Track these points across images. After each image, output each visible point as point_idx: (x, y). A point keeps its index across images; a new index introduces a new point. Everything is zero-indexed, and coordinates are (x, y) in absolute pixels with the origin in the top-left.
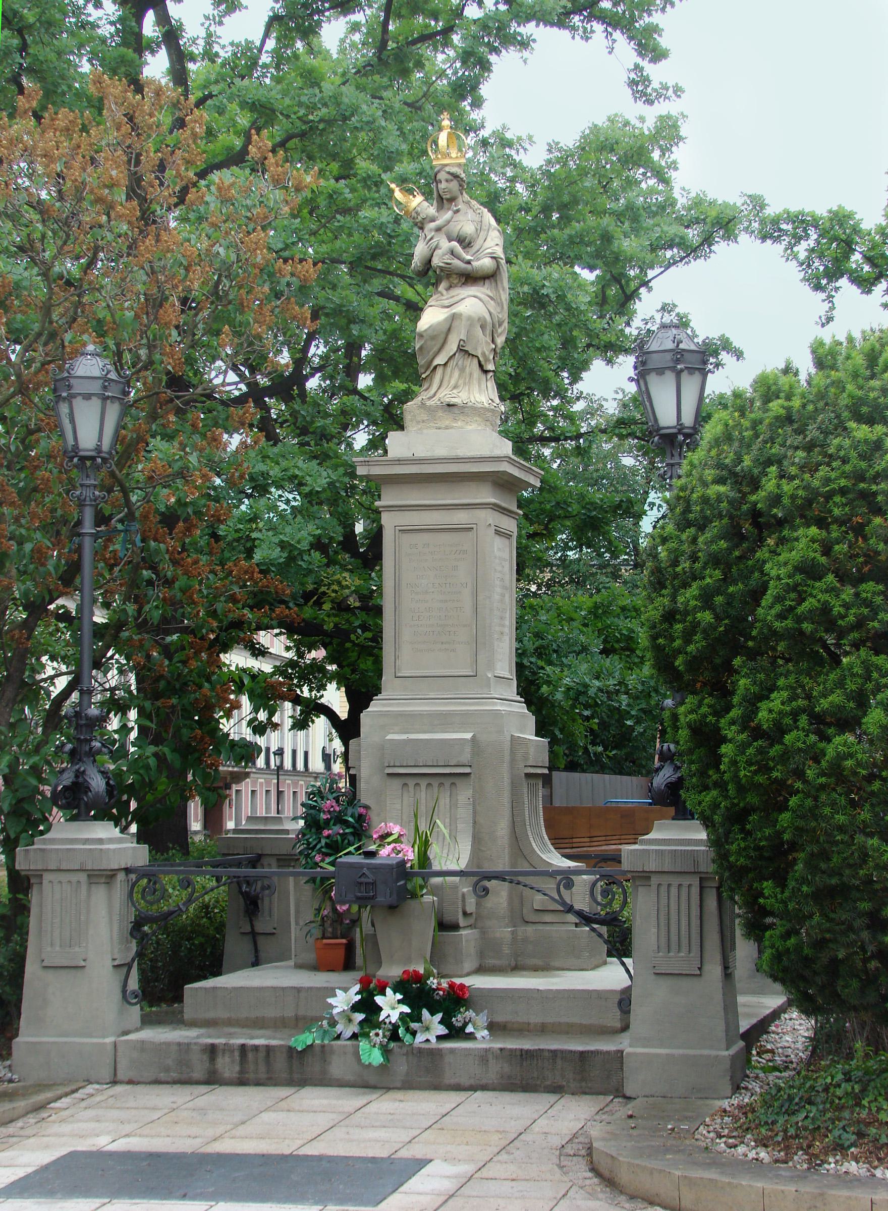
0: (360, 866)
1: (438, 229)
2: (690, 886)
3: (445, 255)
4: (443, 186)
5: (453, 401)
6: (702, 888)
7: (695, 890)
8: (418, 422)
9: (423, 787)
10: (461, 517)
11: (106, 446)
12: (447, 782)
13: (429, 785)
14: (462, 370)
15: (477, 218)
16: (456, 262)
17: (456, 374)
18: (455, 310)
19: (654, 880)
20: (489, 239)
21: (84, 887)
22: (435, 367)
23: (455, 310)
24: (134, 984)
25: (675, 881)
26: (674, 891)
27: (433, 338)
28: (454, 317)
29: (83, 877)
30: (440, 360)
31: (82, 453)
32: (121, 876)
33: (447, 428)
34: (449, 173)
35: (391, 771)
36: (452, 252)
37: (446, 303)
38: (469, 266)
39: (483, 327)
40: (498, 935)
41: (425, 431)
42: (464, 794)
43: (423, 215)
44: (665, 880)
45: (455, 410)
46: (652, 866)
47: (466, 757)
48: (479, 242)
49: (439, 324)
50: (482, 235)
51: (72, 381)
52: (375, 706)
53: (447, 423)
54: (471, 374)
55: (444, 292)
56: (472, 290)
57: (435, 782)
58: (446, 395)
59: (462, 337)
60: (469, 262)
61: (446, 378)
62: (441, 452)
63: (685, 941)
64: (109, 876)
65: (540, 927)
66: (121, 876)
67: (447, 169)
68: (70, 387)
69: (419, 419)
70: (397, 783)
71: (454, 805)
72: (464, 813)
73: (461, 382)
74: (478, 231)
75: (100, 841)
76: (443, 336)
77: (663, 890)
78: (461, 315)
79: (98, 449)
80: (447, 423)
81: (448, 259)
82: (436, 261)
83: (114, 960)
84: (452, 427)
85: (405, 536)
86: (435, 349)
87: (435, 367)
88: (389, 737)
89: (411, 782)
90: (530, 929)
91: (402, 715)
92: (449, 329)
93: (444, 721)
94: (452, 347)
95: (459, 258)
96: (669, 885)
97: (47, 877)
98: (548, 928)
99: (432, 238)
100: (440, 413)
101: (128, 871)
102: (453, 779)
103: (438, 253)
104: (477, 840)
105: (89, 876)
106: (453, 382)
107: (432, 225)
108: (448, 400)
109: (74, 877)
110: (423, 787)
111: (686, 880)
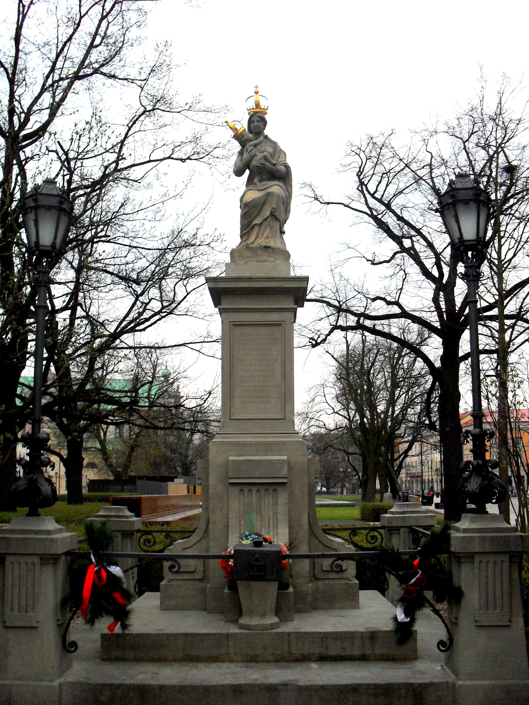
0: (253, 553)
1: (255, 146)
2: (502, 561)
3: (260, 159)
4: (256, 123)
5: (268, 245)
6: (511, 562)
7: (506, 565)
8: (244, 258)
9: (254, 491)
10: (274, 317)
12: (271, 489)
13: (258, 490)
14: (271, 227)
15: (273, 145)
16: (268, 164)
17: (268, 230)
18: (268, 190)
19: (477, 559)
21: (38, 567)
22: (254, 226)
23: (268, 190)
25: (492, 559)
26: (491, 566)
27: (254, 206)
29: (36, 560)
30: (257, 221)
31: (41, 248)
32: (63, 558)
33: (264, 261)
34: (259, 117)
35: (231, 481)
37: (260, 188)
39: (283, 203)
40: (304, 589)
41: (250, 263)
42: (283, 497)
43: (246, 137)
44: (485, 558)
45: (270, 251)
46: (476, 547)
47: (284, 472)
49: (259, 198)
50: (277, 154)
51: (38, 196)
52: (217, 438)
53: (264, 258)
54: (276, 231)
55: (258, 183)
56: (276, 182)
57: (262, 489)
58: (262, 241)
59: (274, 206)
60: (274, 165)
61: (261, 232)
63: (499, 602)
64: (54, 559)
65: (327, 582)
66: (63, 558)
67: (258, 114)
68: (36, 200)
69: (245, 256)
71: (276, 504)
73: (270, 235)
75: (49, 532)
76: (260, 206)
77: (491, 566)
79: (53, 245)
80: (264, 258)
82: (254, 163)
83: (58, 620)
84: (268, 261)
85: (238, 329)
86: (255, 214)
87: (254, 226)
88: (231, 458)
89: (246, 489)
90: (320, 583)
91: (238, 444)
92: (264, 203)
93: (268, 447)
94: (267, 212)
95: (270, 162)
96: (488, 562)
97: (9, 559)
98: (332, 582)
100: (260, 252)
101: (67, 554)
102: (275, 486)
105: (41, 558)
106: (265, 235)
108: (264, 244)
109: (30, 560)
110: (254, 491)
111: (499, 558)
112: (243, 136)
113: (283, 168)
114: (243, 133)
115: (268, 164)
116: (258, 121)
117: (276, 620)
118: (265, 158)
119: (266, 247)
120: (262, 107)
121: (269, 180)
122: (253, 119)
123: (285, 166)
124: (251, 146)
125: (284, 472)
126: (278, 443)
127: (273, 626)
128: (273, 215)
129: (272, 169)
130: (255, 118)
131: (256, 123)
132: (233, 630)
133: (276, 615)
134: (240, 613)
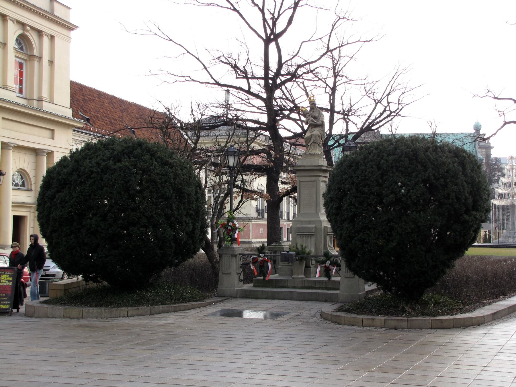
1: (309, 115)
10: (313, 178)
11: (235, 165)
24: (242, 277)
28: (312, 135)
29: (230, 255)
30: (309, 144)
36: (312, 120)
39: (319, 137)
42: (313, 239)
47: (313, 230)
62: (309, 164)
70: (299, 236)
71: (311, 241)
72: (313, 242)
79: (233, 166)
85: (302, 183)
93: (310, 222)
94: (312, 141)
101: (240, 254)
104: (316, 248)
117: (303, 276)
119: (311, 154)
125: (313, 230)
126: (313, 221)
127: (303, 278)
128: (313, 142)
132: (291, 279)
133: (304, 274)
134: (293, 274)
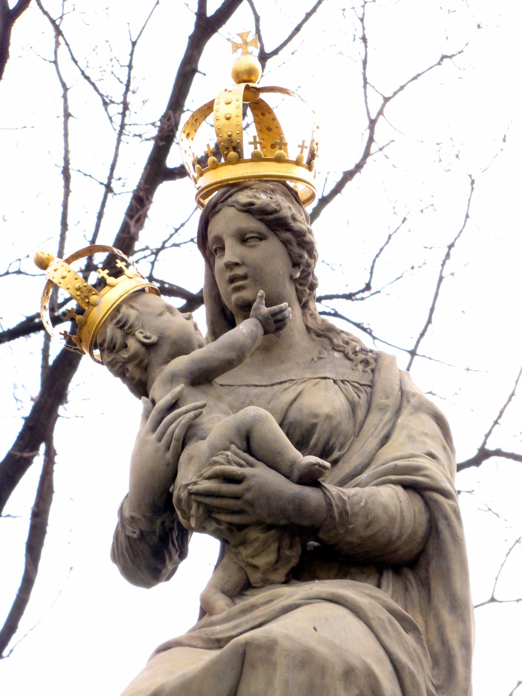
1: (202, 378)
3: (215, 450)
15: (357, 375)
16: (261, 474)
20: (398, 438)
34: (248, 209)
38: (311, 494)
48: (368, 442)
60: (311, 478)
67: (243, 197)
74: (359, 412)
78: (270, 647)
81: (231, 462)
99: (173, 406)
103: (198, 448)
107: (180, 363)
112: (125, 328)
113: (389, 497)
114: (130, 313)
115: (261, 474)
116: (243, 238)
118: (248, 441)
120: (292, 154)
121: (299, 574)
122: (217, 227)
123: (409, 487)
124: (173, 379)
129: (300, 505)
130: (228, 221)
131: (232, 252)
